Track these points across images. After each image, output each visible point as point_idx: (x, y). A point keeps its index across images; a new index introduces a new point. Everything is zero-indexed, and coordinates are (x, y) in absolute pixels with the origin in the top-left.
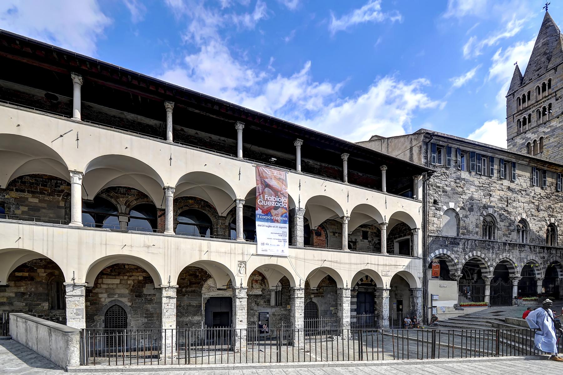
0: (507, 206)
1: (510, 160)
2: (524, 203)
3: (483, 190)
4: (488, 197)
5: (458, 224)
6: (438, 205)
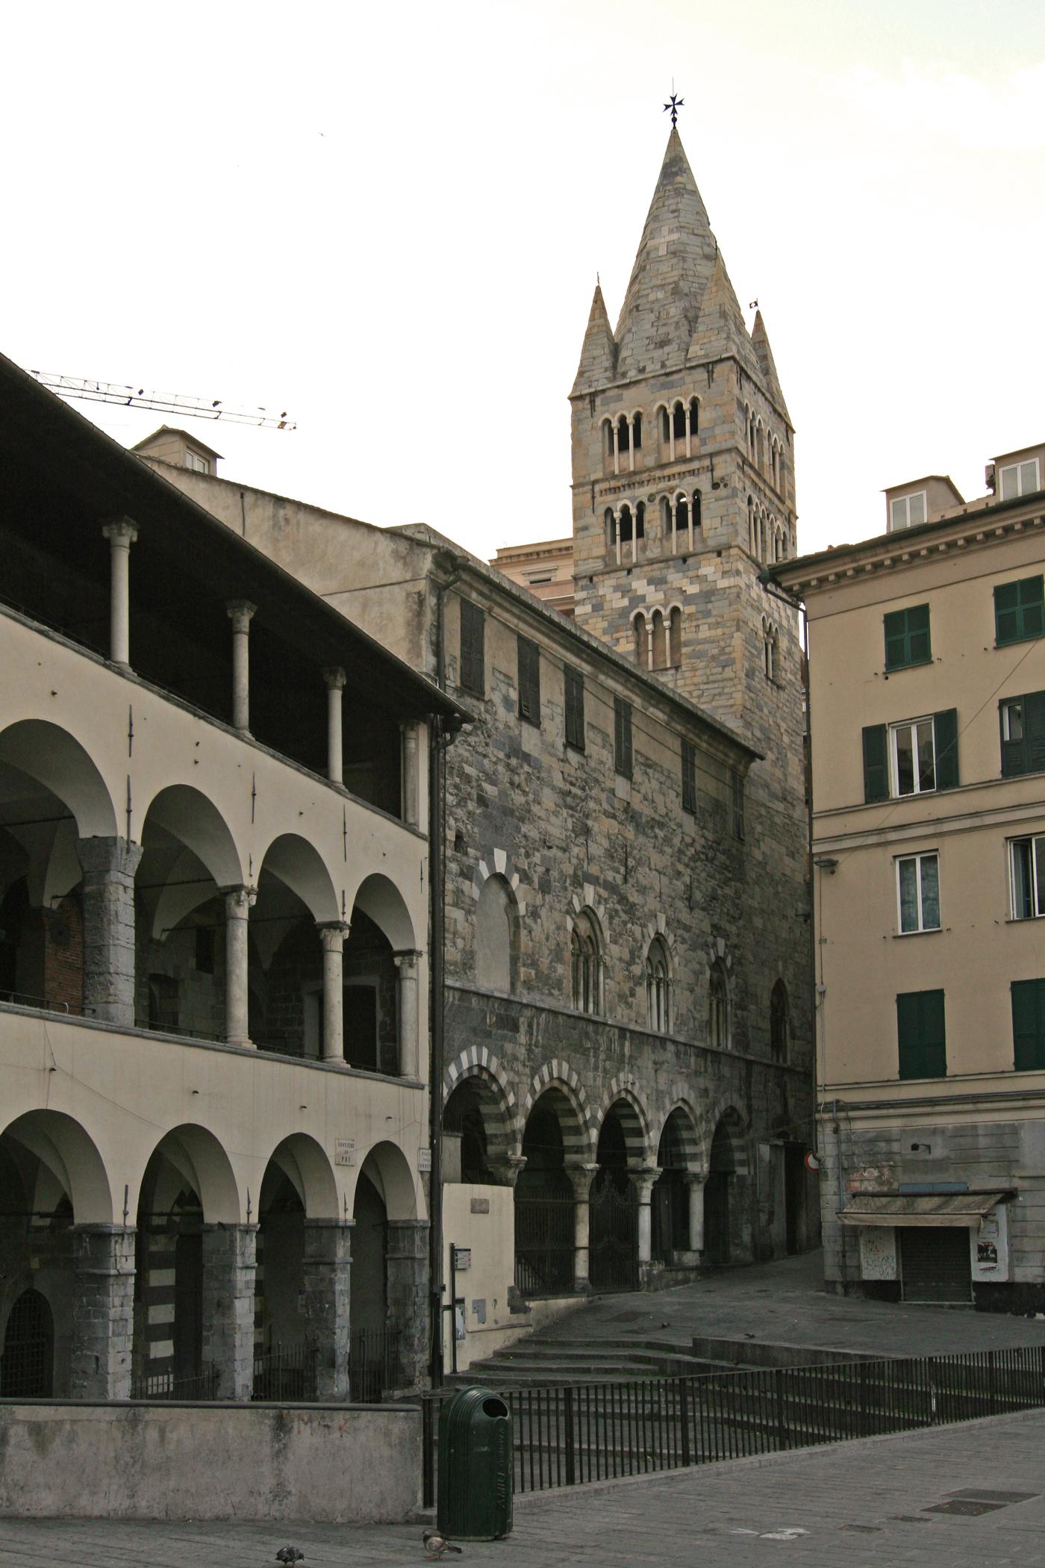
1: (630, 698)
2: (660, 873)
3: (572, 808)
4: (581, 840)
5: (514, 944)
6: (466, 854)
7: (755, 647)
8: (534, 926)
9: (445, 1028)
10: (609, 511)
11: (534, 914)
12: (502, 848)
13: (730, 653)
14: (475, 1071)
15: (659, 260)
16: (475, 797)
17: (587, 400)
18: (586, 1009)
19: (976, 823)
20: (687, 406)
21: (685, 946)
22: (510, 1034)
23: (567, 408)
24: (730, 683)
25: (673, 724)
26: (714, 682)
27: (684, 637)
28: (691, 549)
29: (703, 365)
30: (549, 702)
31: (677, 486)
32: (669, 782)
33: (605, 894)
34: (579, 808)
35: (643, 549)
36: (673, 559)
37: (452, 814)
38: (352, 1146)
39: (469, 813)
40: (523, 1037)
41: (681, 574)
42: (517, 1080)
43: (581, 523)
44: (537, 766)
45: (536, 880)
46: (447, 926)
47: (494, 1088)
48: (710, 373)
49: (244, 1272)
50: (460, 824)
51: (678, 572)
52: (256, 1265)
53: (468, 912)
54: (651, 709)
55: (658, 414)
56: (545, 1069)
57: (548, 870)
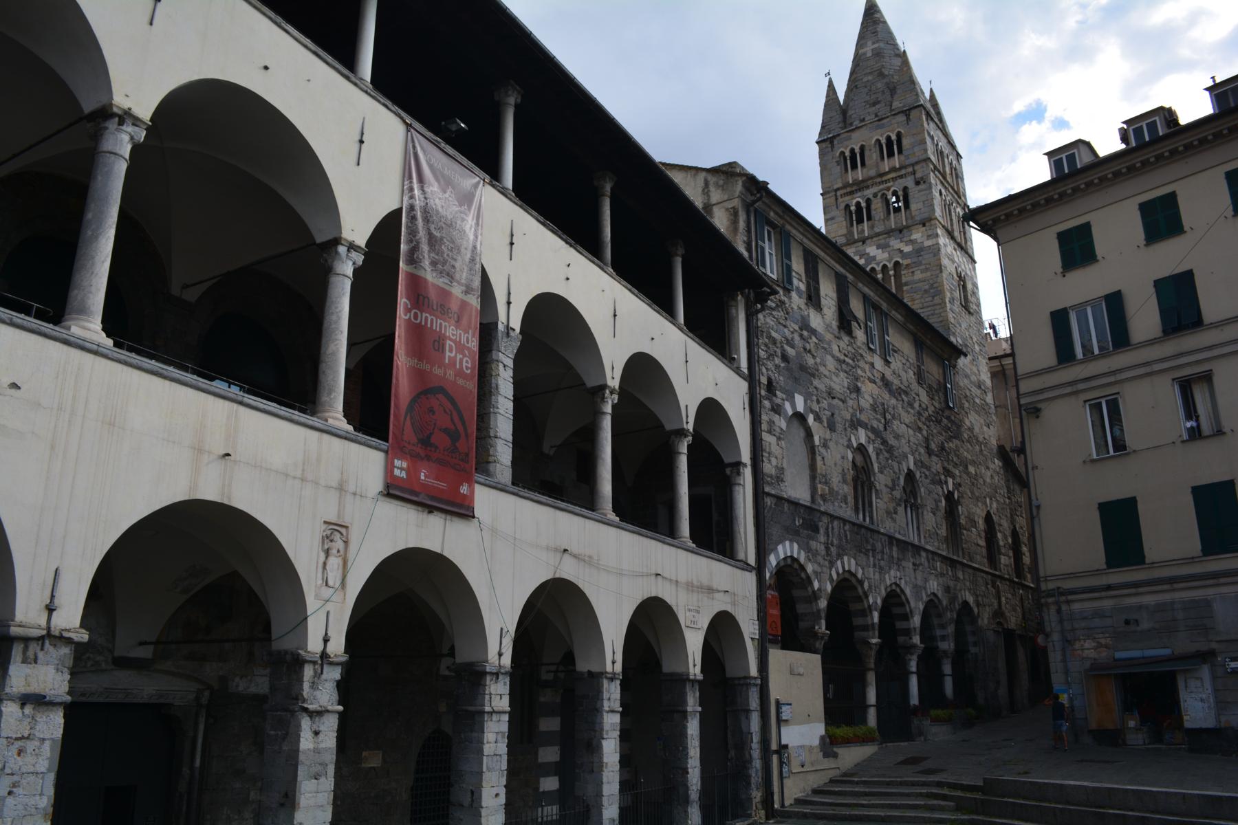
0: (885, 429)
2: (907, 426)
3: (846, 372)
4: (854, 396)
5: (813, 467)
7: (952, 284)
8: (825, 454)
9: (766, 526)
10: (847, 207)
11: (825, 445)
12: (800, 394)
13: (937, 288)
14: (789, 561)
15: (867, 59)
16: (780, 355)
17: (828, 143)
18: (864, 520)
19: (1148, 371)
20: (894, 137)
21: (928, 481)
22: (813, 534)
23: (816, 148)
24: (938, 307)
25: (908, 325)
26: (928, 307)
27: (904, 280)
28: (904, 223)
29: (902, 112)
30: (826, 295)
31: (892, 186)
32: (908, 363)
33: (873, 437)
34: (851, 373)
35: (872, 227)
36: (892, 231)
37: (763, 364)
38: (698, 612)
39: (776, 366)
40: (822, 537)
41: (899, 240)
42: (819, 570)
43: (828, 217)
44: (820, 339)
45: (825, 420)
46: (764, 447)
47: (803, 575)
48: (908, 116)
49: (610, 715)
50: (770, 373)
51: (896, 239)
52: (621, 709)
53: (779, 439)
54: (893, 312)
55: (875, 144)
56: (839, 563)
57: (833, 415)
